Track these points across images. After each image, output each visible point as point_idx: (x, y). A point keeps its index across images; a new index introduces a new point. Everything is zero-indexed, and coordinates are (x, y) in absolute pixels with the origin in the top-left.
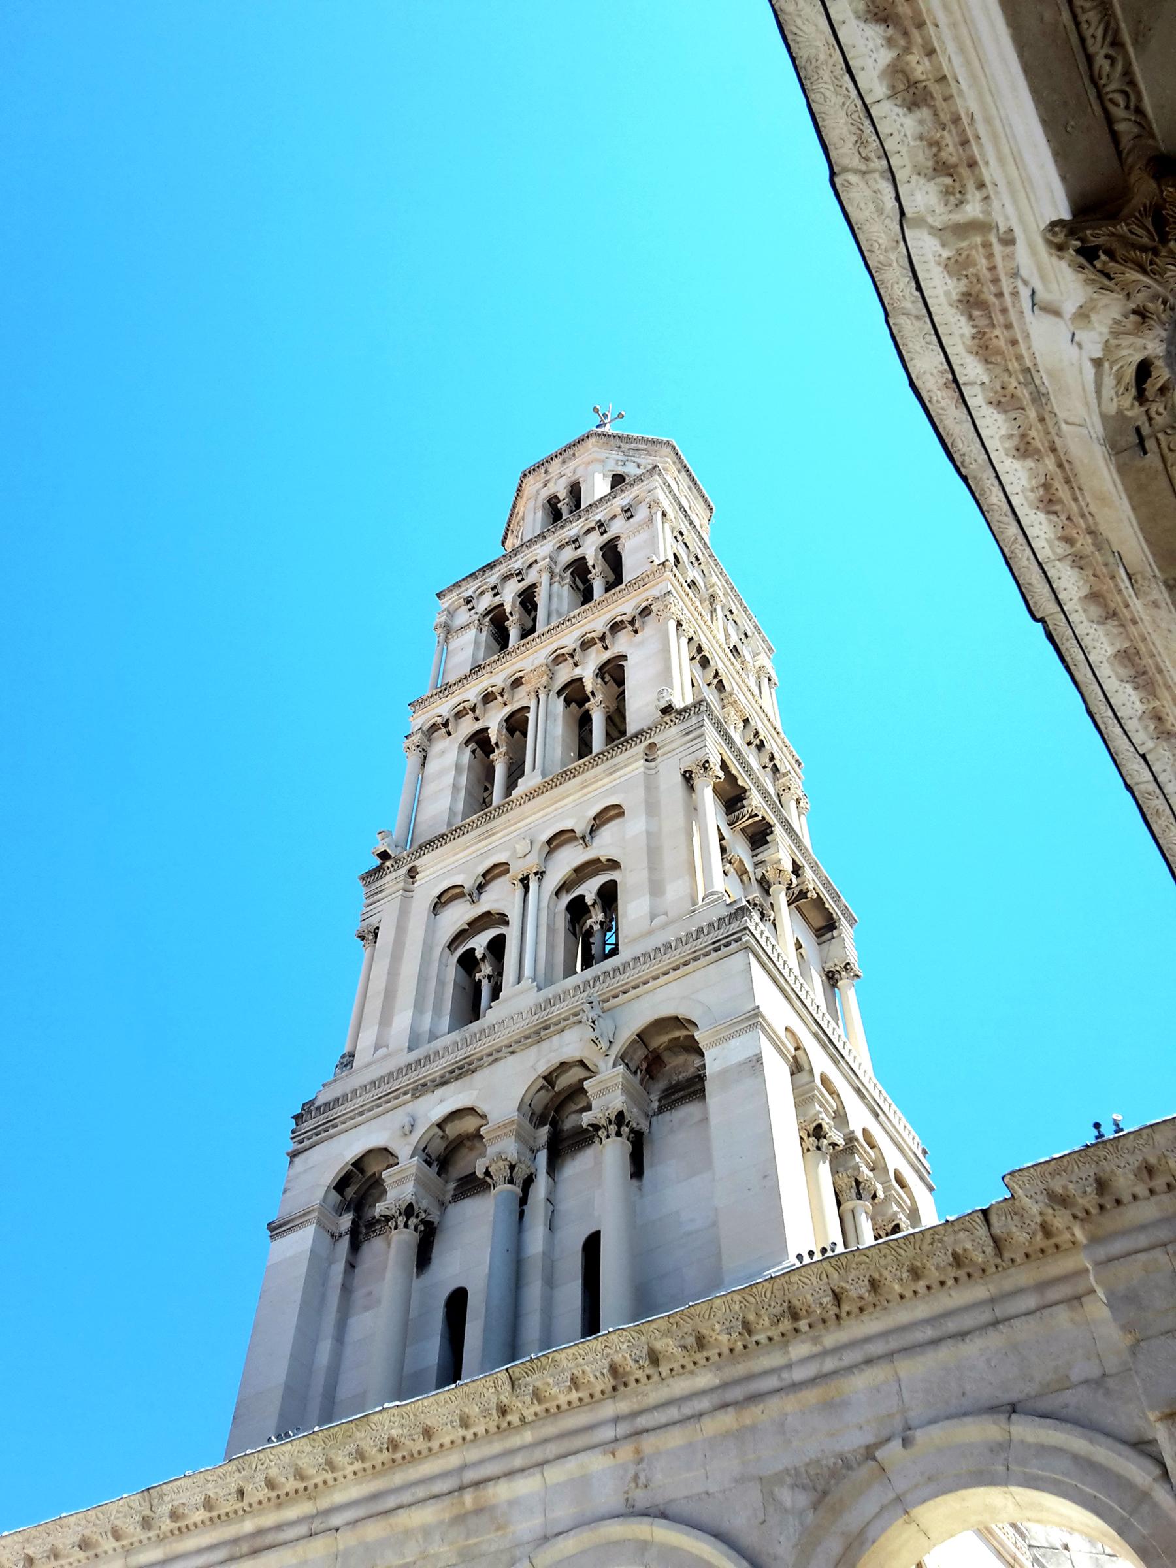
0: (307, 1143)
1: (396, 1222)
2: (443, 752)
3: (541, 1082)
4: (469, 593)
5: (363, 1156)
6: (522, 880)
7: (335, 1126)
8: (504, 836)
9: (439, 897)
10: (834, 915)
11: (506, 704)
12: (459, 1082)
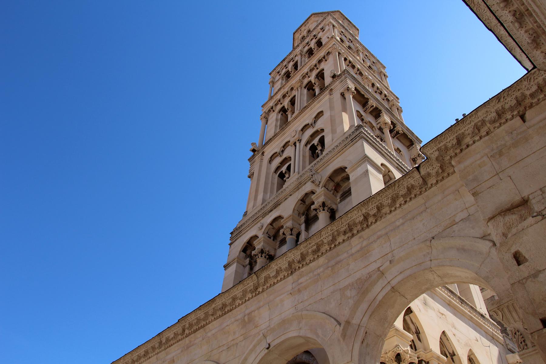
1: (258, 256)
2: (272, 117)
3: (300, 202)
4: (279, 70)
6: (294, 144)
8: (288, 133)
9: (271, 158)
10: (412, 140)
11: (289, 96)
12: (275, 210)
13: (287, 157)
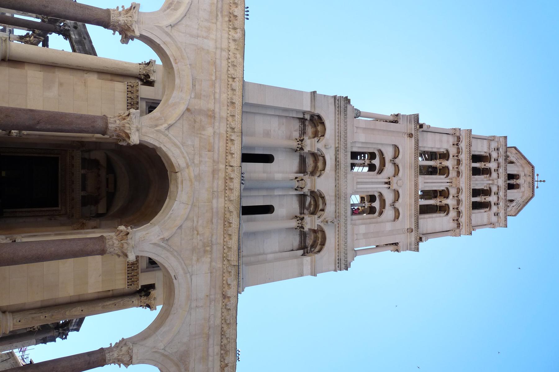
0: (337, 102)
5: (325, 126)
6: (390, 182)
7: (338, 114)
8: (407, 174)
9: (398, 147)
11: (453, 168)
13: (384, 167)
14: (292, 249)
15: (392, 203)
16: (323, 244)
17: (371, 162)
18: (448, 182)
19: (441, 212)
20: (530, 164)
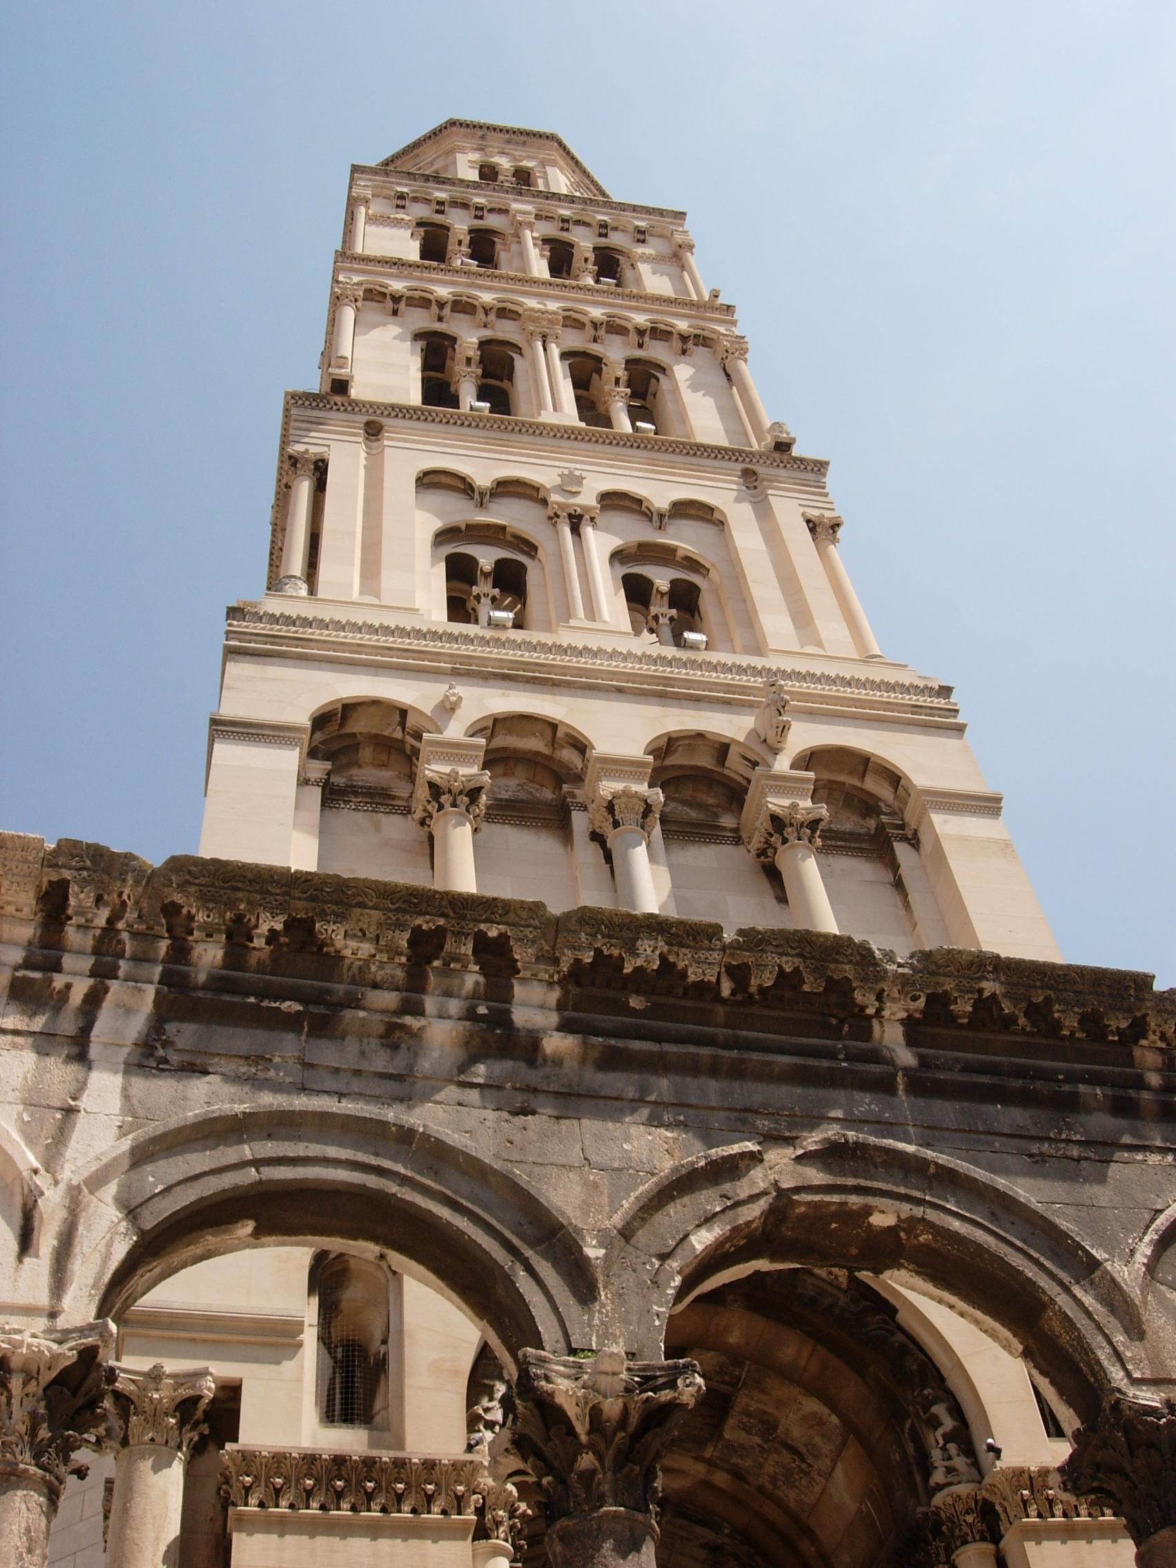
6: (570, 516)
9: (427, 473)
11: (485, 326)
14: (889, 888)
15: (651, 520)
16: (862, 763)
17: (486, 575)
18: (545, 350)
19: (651, 390)
20: (440, 131)
